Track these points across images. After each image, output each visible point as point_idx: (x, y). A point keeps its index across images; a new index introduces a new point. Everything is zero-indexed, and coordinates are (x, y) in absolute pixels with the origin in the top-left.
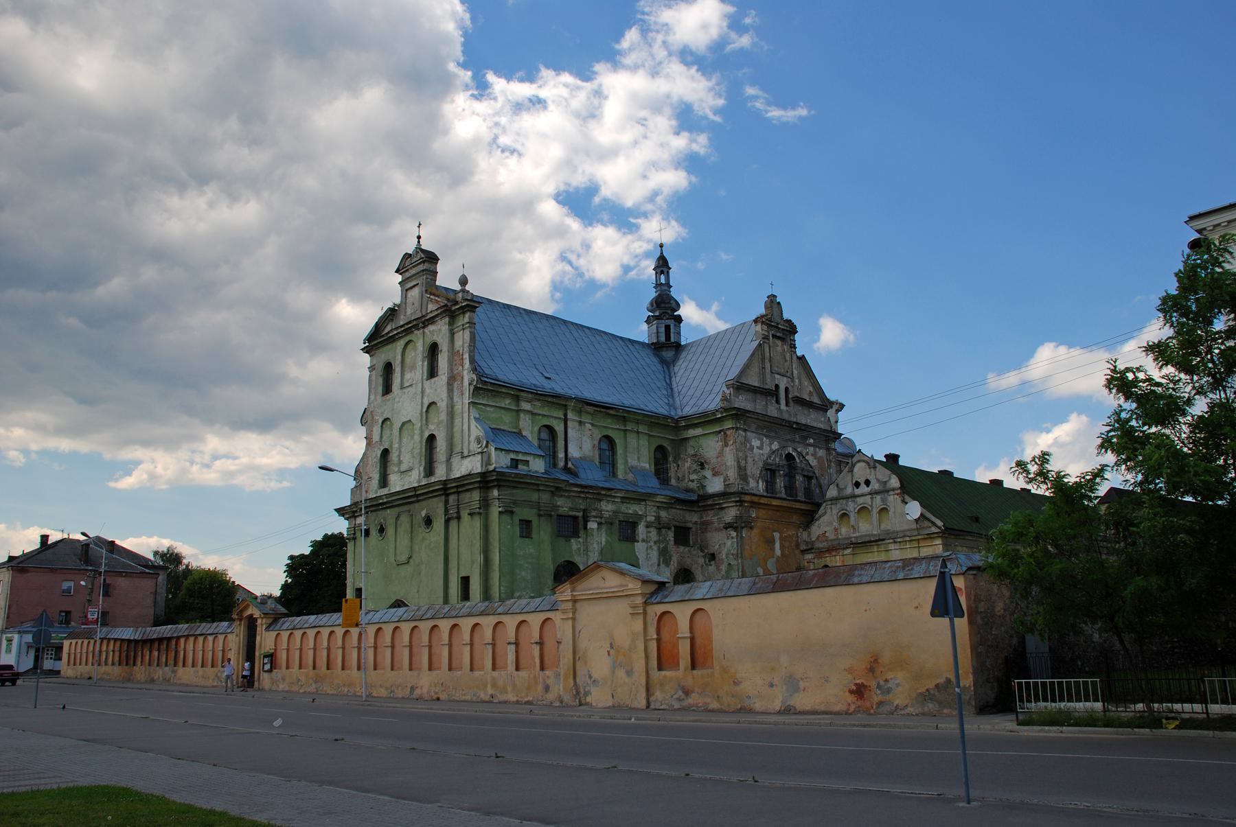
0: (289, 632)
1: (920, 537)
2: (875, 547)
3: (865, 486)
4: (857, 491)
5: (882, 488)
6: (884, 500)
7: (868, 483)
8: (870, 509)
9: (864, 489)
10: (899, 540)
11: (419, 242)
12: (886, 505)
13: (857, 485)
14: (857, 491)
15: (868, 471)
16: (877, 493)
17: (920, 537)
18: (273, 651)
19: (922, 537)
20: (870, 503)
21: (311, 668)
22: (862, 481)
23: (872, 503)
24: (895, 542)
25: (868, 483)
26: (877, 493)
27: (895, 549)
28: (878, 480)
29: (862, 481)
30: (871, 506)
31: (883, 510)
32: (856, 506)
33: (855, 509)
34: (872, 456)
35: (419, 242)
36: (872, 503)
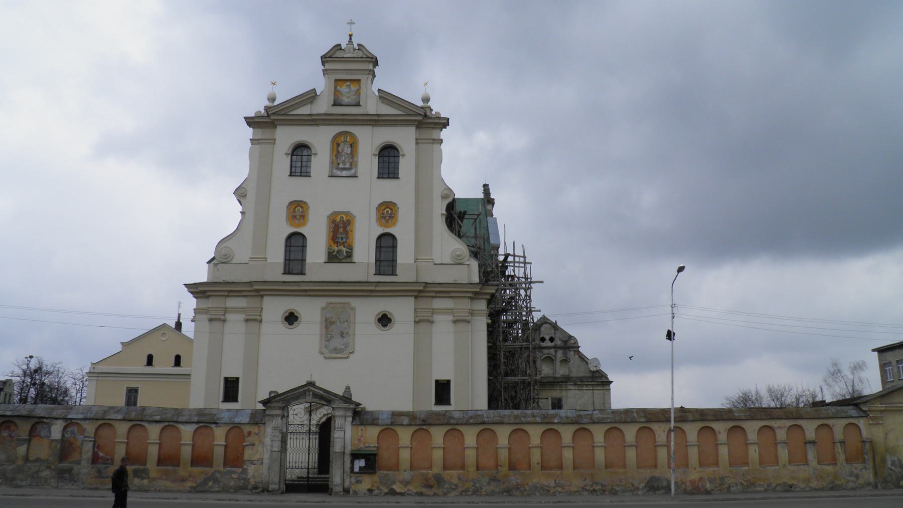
0: (414, 428)
1: (593, 383)
2: (558, 387)
3: (549, 342)
4: (543, 344)
5: (563, 345)
6: (565, 354)
7: (552, 340)
8: (554, 358)
9: (549, 344)
10: (579, 383)
11: (350, 39)
12: (567, 357)
13: (543, 340)
14: (543, 344)
15: (553, 331)
16: (560, 348)
17: (593, 383)
18: (375, 449)
19: (596, 383)
20: (554, 354)
21: (472, 469)
22: (547, 338)
23: (556, 354)
24: (575, 385)
25: (552, 340)
26: (560, 348)
27: (574, 390)
28: (560, 340)
29: (547, 338)
30: (555, 356)
31: (565, 361)
32: (542, 355)
33: (541, 357)
34: (556, 321)
35: (350, 39)
36: (556, 354)
